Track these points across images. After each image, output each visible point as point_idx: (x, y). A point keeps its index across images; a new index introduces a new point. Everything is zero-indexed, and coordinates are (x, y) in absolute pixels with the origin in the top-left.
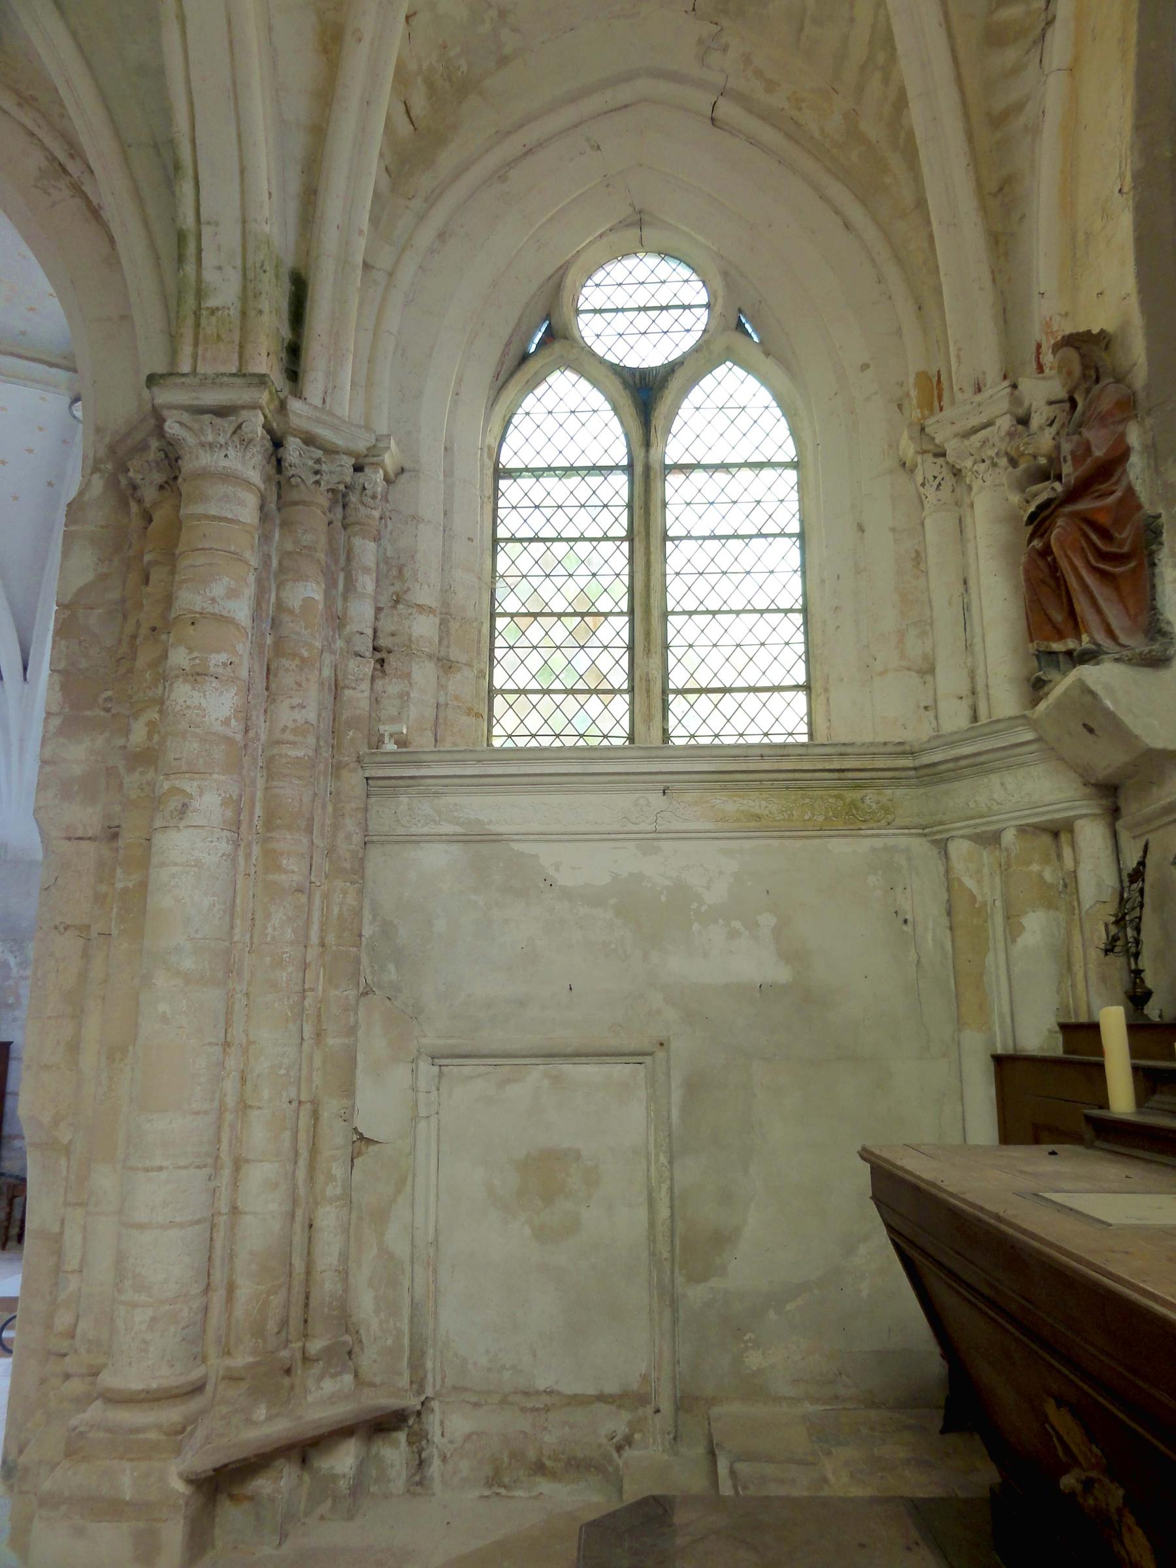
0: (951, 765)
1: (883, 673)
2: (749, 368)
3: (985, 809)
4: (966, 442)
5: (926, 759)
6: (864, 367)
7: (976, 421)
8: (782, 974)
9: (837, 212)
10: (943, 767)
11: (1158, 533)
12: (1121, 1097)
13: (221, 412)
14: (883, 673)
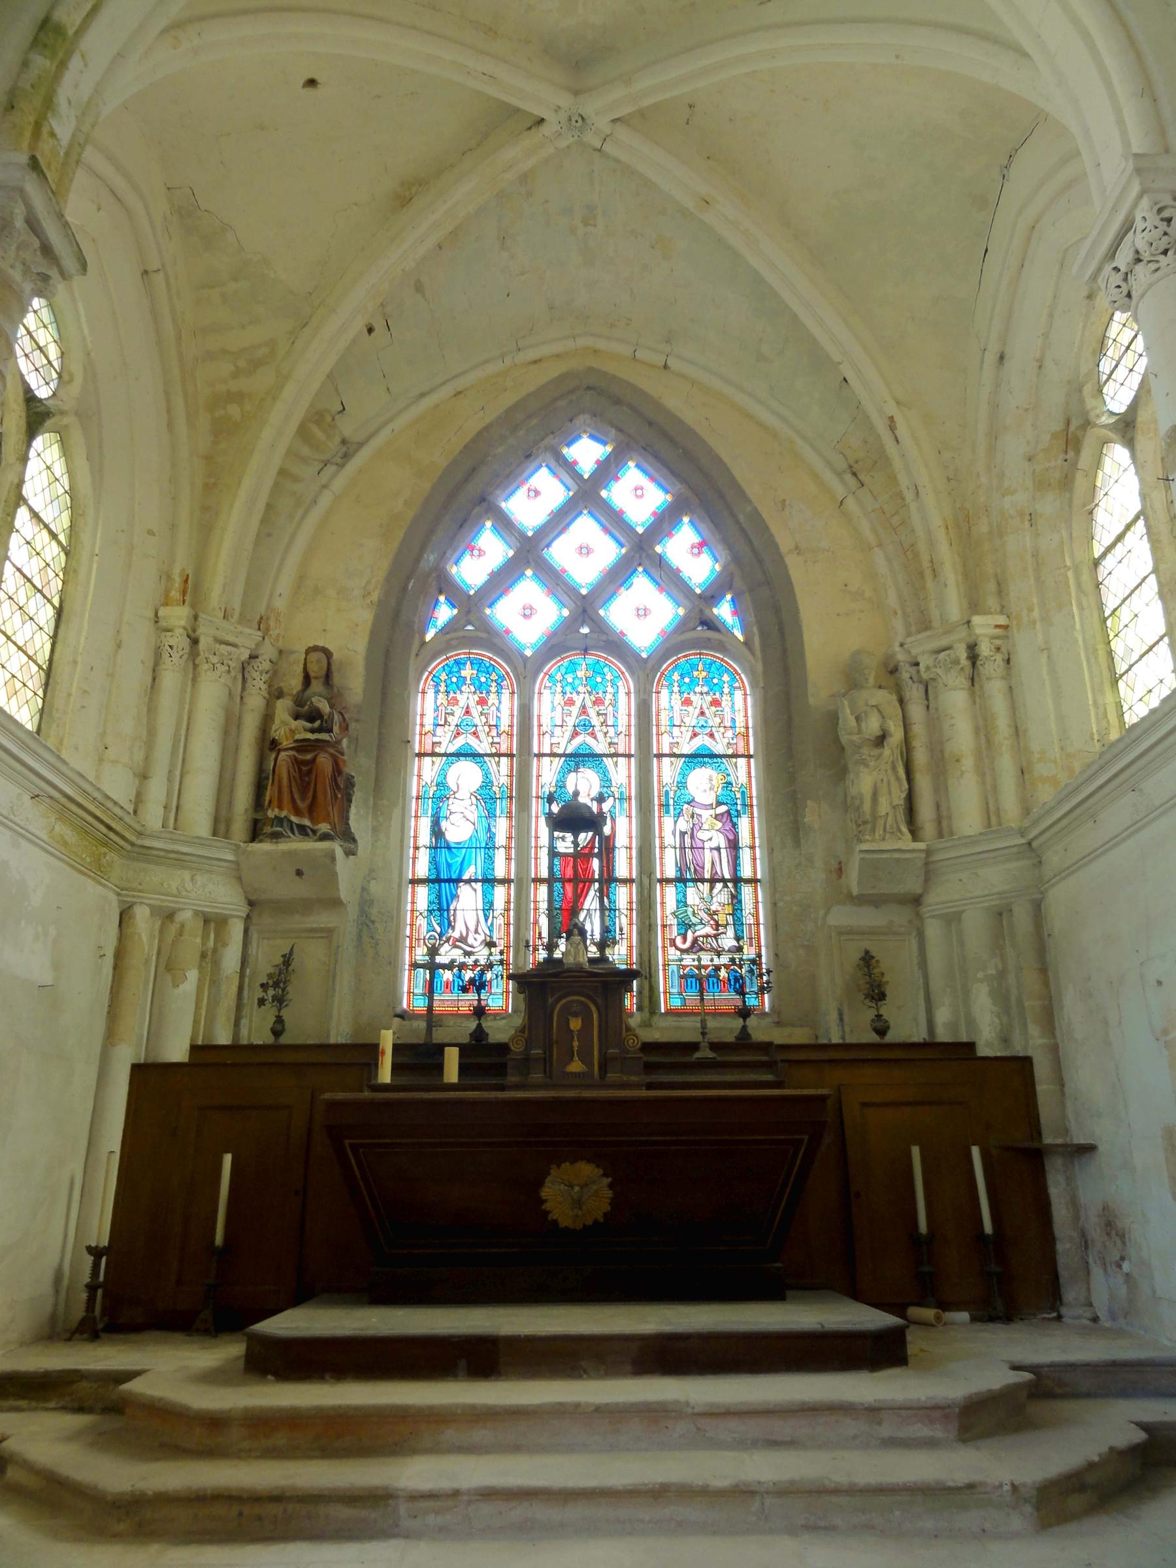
0: (162, 854)
1: (115, 762)
2: (66, 452)
3: (175, 892)
4: (217, 646)
5: (147, 843)
6: (151, 533)
7: (231, 638)
8: (47, 978)
9: (169, 412)
10: (155, 852)
11: (353, 785)
12: (385, 1075)
13: (47, 250)
14: (115, 762)
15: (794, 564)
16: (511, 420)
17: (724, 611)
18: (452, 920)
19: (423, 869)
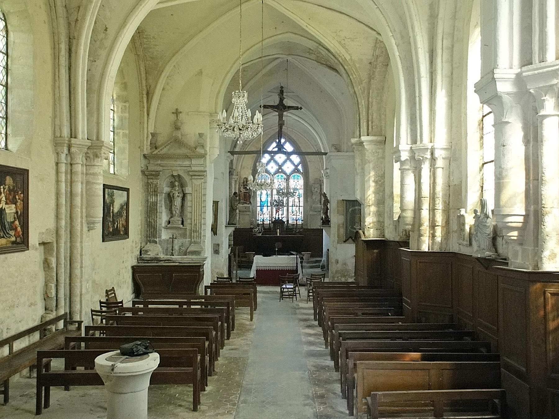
15: (309, 163)
16: (270, 139)
17: (300, 167)
18: (265, 216)
19: (259, 205)
